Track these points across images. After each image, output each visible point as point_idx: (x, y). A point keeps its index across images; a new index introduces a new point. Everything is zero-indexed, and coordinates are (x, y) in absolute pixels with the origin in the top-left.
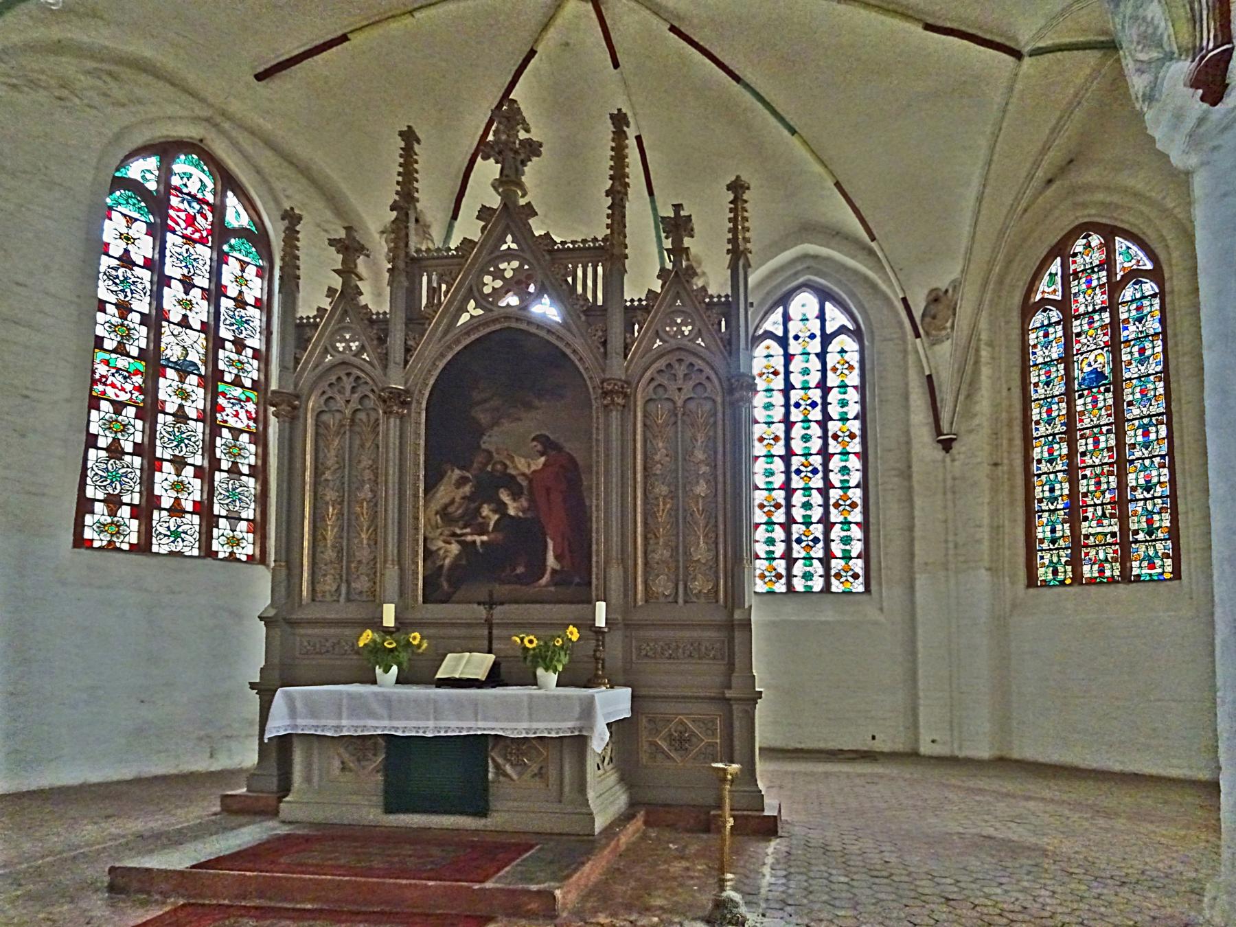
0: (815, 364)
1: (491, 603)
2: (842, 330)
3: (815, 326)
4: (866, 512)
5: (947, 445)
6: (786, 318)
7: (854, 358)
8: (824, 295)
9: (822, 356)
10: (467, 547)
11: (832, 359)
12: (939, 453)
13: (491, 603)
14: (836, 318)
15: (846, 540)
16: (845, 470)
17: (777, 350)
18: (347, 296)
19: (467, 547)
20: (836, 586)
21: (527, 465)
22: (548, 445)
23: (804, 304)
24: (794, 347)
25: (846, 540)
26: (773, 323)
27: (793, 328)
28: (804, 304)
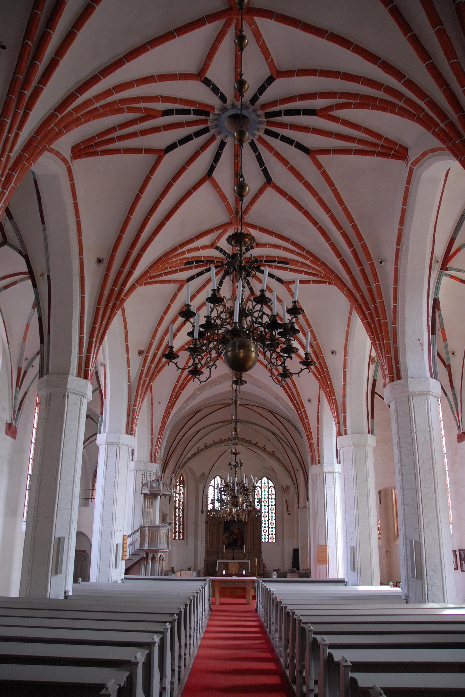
0: (267, 493)
1: (233, 550)
2: (271, 486)
3: (267, 485)
4: (276, 525)
5: (289, 514)
6: (261, 483)
7: (274, 492)
8: (268, 479)
9: (268, 492)
10: (229, 542)
11: (270, 492)
12: (288, 515)
13: (233, 550)
14: (271, 484)
15: (272, 531)
16: (272, 516)
17: (259, 489)
18: (214, 507)
19: (229, 542)
20: (270, 541)
21: (236, 531)
22: (239, 529)
23: (265, 480)
24: (263, 489)
25: (272, 531)
26: (259, 484)
27: (263, 485)
28: (265, 480)
